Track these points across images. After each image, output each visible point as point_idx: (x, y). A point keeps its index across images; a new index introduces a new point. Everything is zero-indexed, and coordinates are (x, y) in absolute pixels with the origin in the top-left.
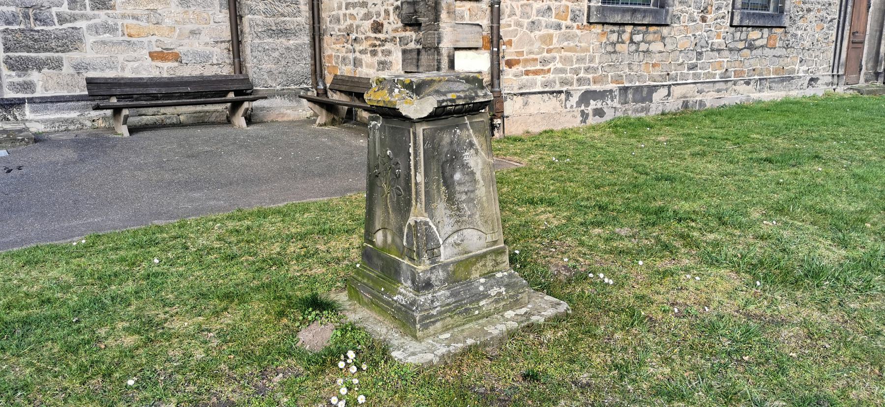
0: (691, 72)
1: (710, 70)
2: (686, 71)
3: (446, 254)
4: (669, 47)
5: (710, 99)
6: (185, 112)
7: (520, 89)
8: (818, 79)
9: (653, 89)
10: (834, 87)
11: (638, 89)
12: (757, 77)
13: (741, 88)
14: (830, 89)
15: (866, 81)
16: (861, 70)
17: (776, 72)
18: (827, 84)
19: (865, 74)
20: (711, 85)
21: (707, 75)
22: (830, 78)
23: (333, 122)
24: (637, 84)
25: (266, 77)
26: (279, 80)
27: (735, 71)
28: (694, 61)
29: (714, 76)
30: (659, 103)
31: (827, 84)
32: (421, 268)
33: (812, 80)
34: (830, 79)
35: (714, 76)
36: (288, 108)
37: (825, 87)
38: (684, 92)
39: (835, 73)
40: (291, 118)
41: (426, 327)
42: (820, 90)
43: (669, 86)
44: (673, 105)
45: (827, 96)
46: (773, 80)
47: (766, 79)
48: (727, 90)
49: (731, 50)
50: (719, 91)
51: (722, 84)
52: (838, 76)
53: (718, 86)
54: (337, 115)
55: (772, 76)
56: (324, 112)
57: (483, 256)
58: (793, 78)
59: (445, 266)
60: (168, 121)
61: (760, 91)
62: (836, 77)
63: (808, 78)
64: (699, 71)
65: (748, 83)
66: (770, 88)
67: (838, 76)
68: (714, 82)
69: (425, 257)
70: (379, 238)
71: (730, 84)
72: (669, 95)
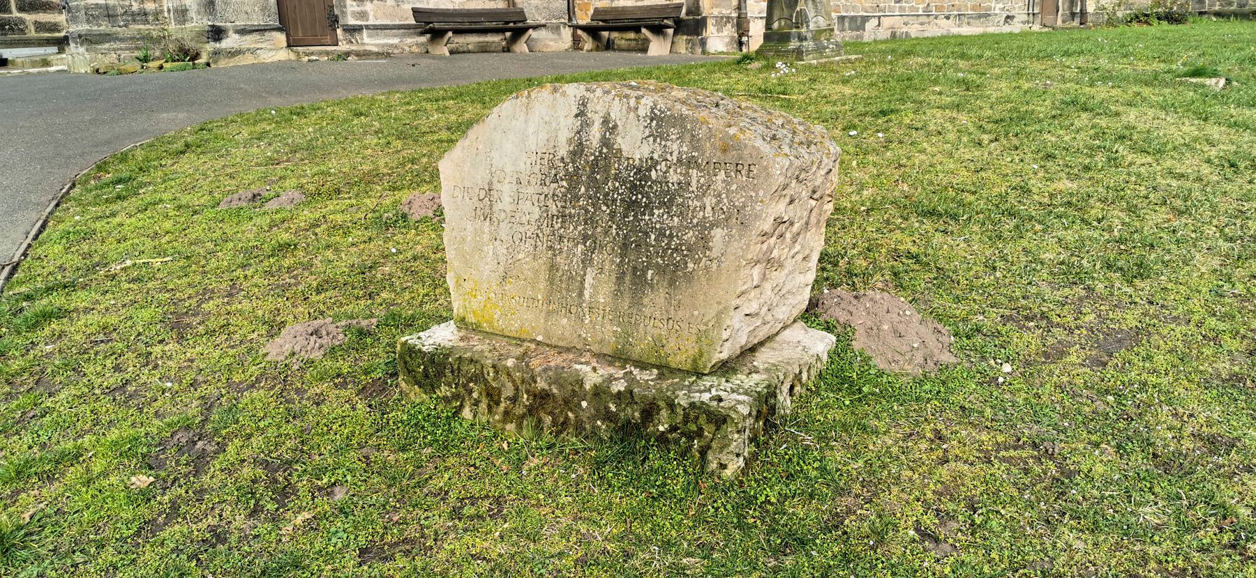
0: (898, 5)
1: (914, 4)
3: (812, 26)
5: (914, 30)
6: (473, 40)
7: (759, 13)
8: (1013, 17)
9: (865, 19)
10: (1030, 25)
11: (853, 19)
12: (956, 13)
13: (942, 22)
14: (1026, 27)
15: (1064, 22)
16: (1058, 11)
17: (973, 8)
18: (1024, 23)
19: (1062, 15)
20: (915, 18)
21: (912, 8)
22: (1026, 16)
23: (597, 49)
24: (852, 14)
25: (534, 11)
26: (543, 14)
27: (936, 6)
29: (917, 10)
30: (871, 32)
31: (1024, 23)
32: (803, 30)
33: (1008, 17)
34: (1025, 18)
35: (917, 10)
36: (551, 40)
37: (1022, 25)
38: (892, 23)
39: (1031, 11)
40: (553, 50)
41: (807, 55)
42: (1016, 27)
43: (879, 17)
44: (883, 34)
45: (1023, 34)
46: (971, 17)
47: (964, 15)
48: (929, 23)
50: (922, 24)
51: (925, 17)
52: (1034, 14)
53: (921, 19)
54: (600, 42)
55: (970, 12)
56: (591, 39)
57: (825, 30)
58: (989, 15)
59: (812, 31)
60: (461, 49)
62: (1031, 15)
63: (1005, 16)
65: (948, 18)
66: (968, 23)
67: (1034, 14)
68: (918, 16)
69: (805, 25)
70: (776, 25)
71: (932, 18)
72: (879, 25)
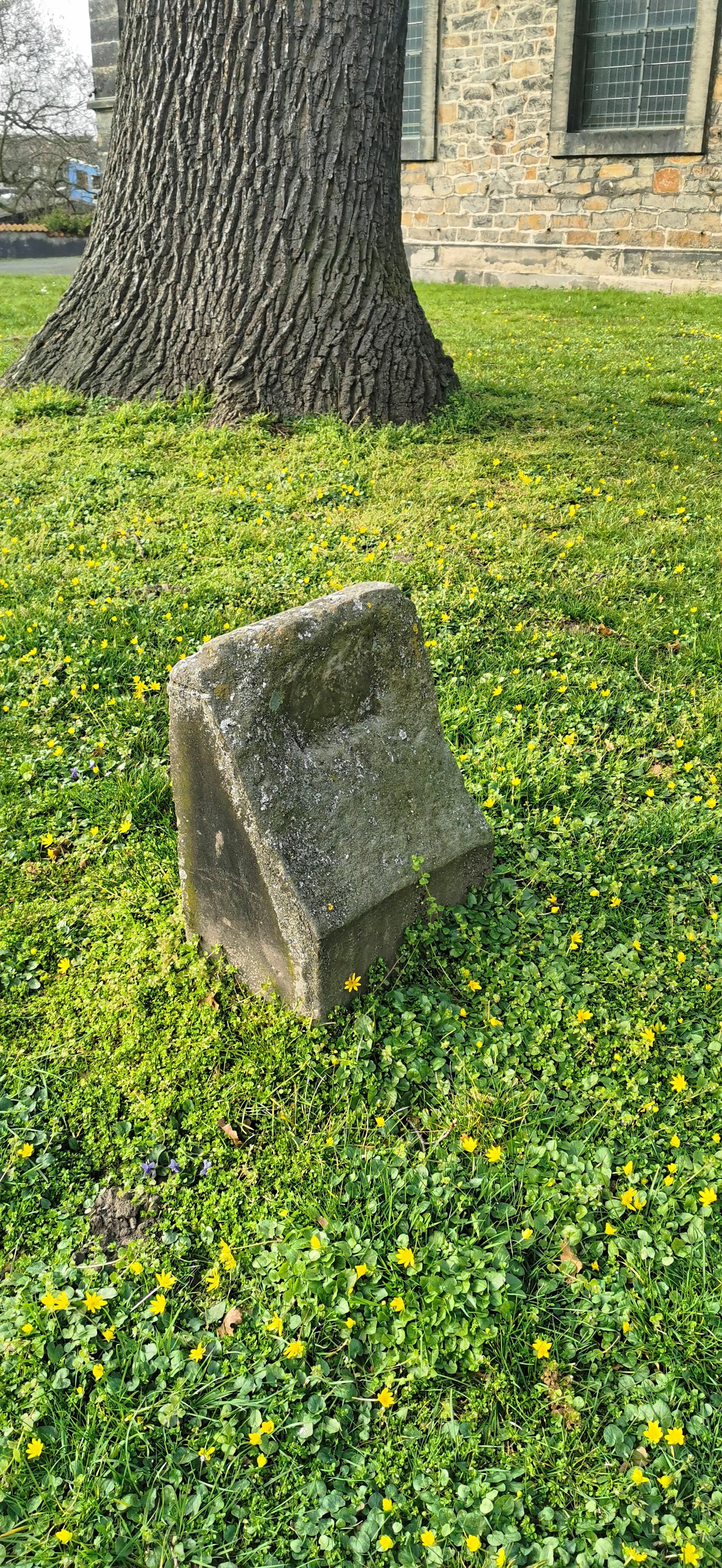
0: (479, 229)
1: (516, 228)
2: (470, 227)
4: (441, 191)
12: (622, 247)
17: (679, 239)
20: (513, 251)
21: (509, 236)
27: (569, 233)
28: (485, 213)
29: (524, 238)
35: (524, 238)
38: (461, 257)
43: (436, 248)
46: (665, 256)
47: (643, 252)
48: (545, 262)
49: (561, 197)
53: (524, 255)
55: (666, 248)
61: (626, 273)
64: (494, 229)
65: (594, 255)
66: (655, 269)
72: (436, 259)
